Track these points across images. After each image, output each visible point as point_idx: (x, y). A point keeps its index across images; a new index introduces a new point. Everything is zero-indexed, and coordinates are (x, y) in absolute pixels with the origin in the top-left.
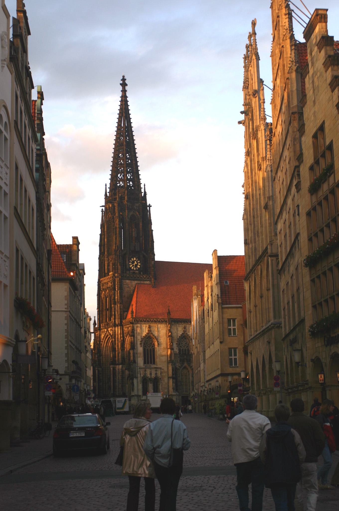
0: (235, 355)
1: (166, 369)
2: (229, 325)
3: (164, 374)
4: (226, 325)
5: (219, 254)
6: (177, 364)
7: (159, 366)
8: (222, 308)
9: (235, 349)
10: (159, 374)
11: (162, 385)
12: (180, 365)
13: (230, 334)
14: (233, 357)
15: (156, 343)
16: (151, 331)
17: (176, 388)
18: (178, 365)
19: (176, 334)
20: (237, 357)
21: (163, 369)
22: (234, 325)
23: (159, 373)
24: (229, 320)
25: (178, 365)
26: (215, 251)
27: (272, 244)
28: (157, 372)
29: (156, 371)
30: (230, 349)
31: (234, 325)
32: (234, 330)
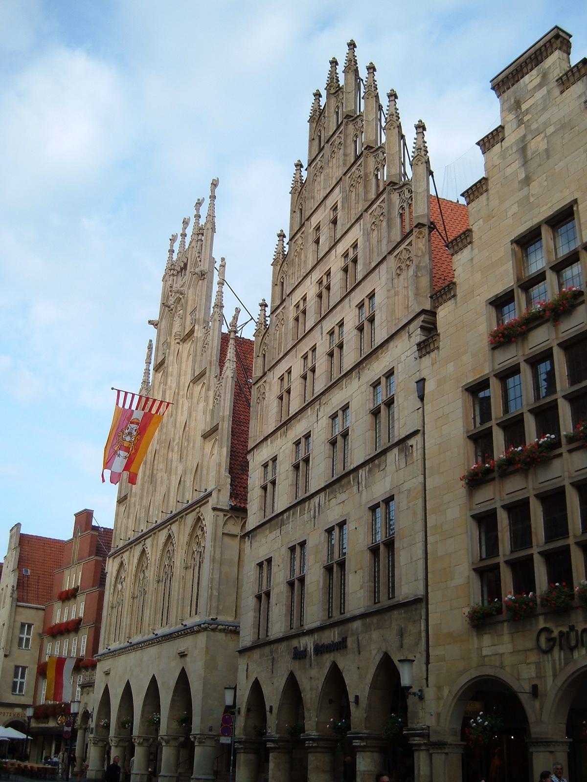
0: (23, 677)
2: (22, 632)
4: (17, 631)
5: (23, 531)
8: (17, 606)
9: (24, 668)
13: (20, 645)
14: (19, 680)
20: (25, 681)
22: (29, 633)
24: (23, 625)
26: (18, 525)
27: (219, 491)
30: (17, 667)
31: (29, 633)
32: (28, 640)
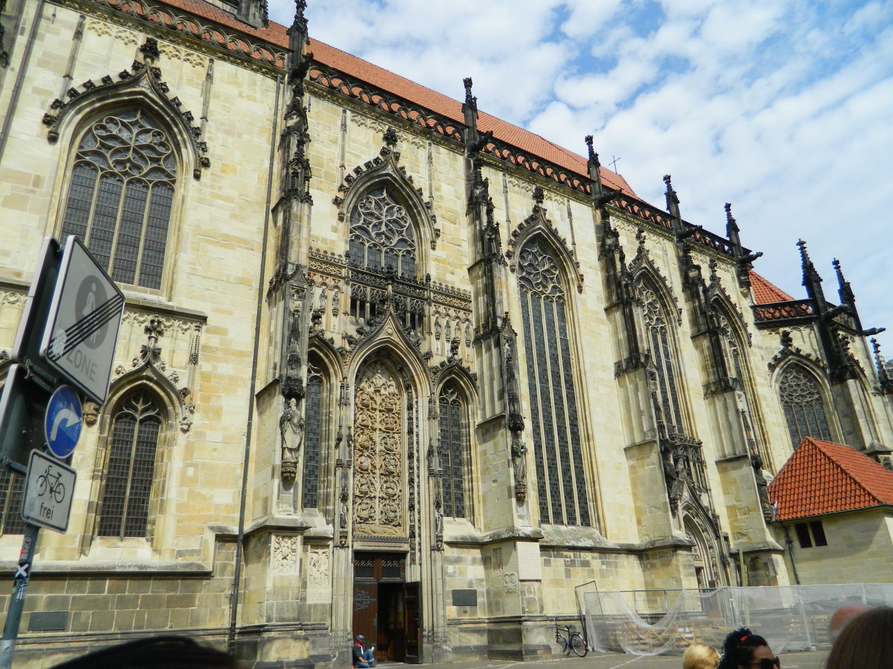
1: (241, 334)
3: (225, 369)
6: (334, 321)
7: (181, 303)
10: (182, 357)
11: (189, 449)
12: (352, 331)
15: (188, 155)
16: (157, 74)
17: (307, 478)
18: (338, 327)
19: (337, 151)
21: (219, 331)
23: (174, 347)
25: (338, 327)
28: (164, 343)
29: (153, 330)
